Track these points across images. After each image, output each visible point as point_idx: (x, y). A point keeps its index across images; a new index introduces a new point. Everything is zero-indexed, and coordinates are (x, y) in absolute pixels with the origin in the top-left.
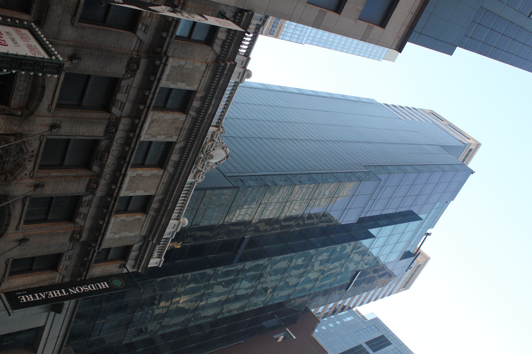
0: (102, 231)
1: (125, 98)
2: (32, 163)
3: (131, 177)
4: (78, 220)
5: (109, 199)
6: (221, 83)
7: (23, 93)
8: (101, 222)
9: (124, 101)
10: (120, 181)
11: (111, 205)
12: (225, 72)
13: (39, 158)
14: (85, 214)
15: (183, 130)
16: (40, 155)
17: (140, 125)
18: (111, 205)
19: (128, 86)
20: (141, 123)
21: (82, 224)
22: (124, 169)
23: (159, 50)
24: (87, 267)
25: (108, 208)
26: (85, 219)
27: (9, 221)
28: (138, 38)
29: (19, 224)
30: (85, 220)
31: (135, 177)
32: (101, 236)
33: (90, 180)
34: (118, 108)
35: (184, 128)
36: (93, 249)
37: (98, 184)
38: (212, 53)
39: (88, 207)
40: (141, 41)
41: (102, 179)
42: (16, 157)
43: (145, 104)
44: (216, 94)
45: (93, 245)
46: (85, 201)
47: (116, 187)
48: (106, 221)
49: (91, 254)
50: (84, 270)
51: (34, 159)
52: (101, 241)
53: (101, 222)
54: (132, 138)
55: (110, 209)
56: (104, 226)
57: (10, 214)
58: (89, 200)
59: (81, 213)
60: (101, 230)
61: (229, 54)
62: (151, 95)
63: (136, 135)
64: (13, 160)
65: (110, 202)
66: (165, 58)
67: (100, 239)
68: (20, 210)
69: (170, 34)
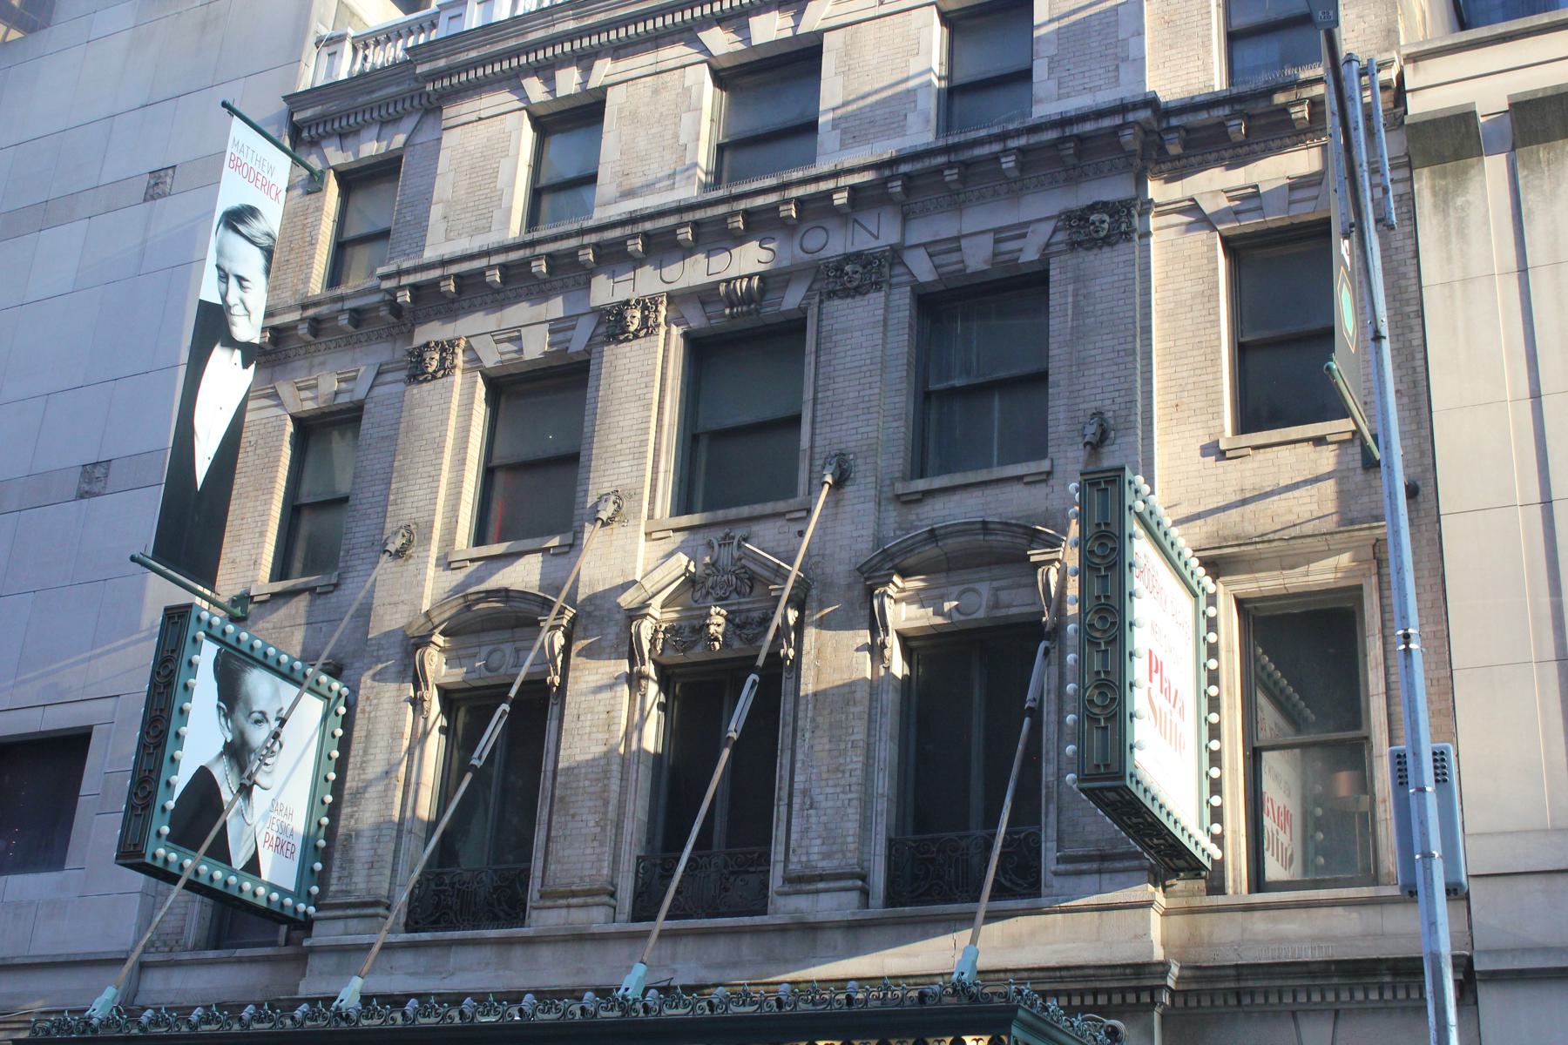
0: (1052, 135)
1: (530, 330)
2: (756, 528)
3: (843, 146)
4: (1030, 253)
5: (896, 187)
6: (473, 54)
7: (508, 649)
8: (1008, 163)
9: (546, 326)
10: (811, 189)
11: (919, 166)
12: (442, 63)
13: (733, 513)
14: (997, 241)
15: (660, 67)
16: (721, 514)
17: (593, 238)
18: (919, 166)
19: (497, 342)
20: (588, 239)
21: (1048, 227)
22: (760, 201)
23: (384, 312)
24: (1280, 98)
25: (939, 171)
26: (1020, 231)
27: (965, 529)
28: (372, 387)
29: (1018, 479)
30: (1027, 224)
31: (844, 132)
32: (1076, 129)
33: (832, 294)
34: (569, 333)
35: (652, 69)
36: (1174, 122)
37: (848, 258)
38: (419, 139)
39: (964, 243)
40: (379, 374)
41: (823, 254)
42: (721, 593)
43: (526, 263)
44: (512, 43)
45: (1128, 137)
46: (936, 267)
47: (837, 190)
48: (996, 147)
49: (1203, 115)
50: (1300, 102)
51: (738, 533)
52: (1099, 114)
53: (1008, 163)
54: (646, 236)
55: (941, 160)
56: (1022, 141)
57: (933, 536)
58: (930, 255)
59: (995, 255)
60: (1055, 144)
61: (404, 87)
62: (495, 260)
63: (628, 230)
64: (734, 598)
65: (908, 178)
66: (386, 284)
67: (1089, 127)
68: (956, 497)
69: (339, 306)
